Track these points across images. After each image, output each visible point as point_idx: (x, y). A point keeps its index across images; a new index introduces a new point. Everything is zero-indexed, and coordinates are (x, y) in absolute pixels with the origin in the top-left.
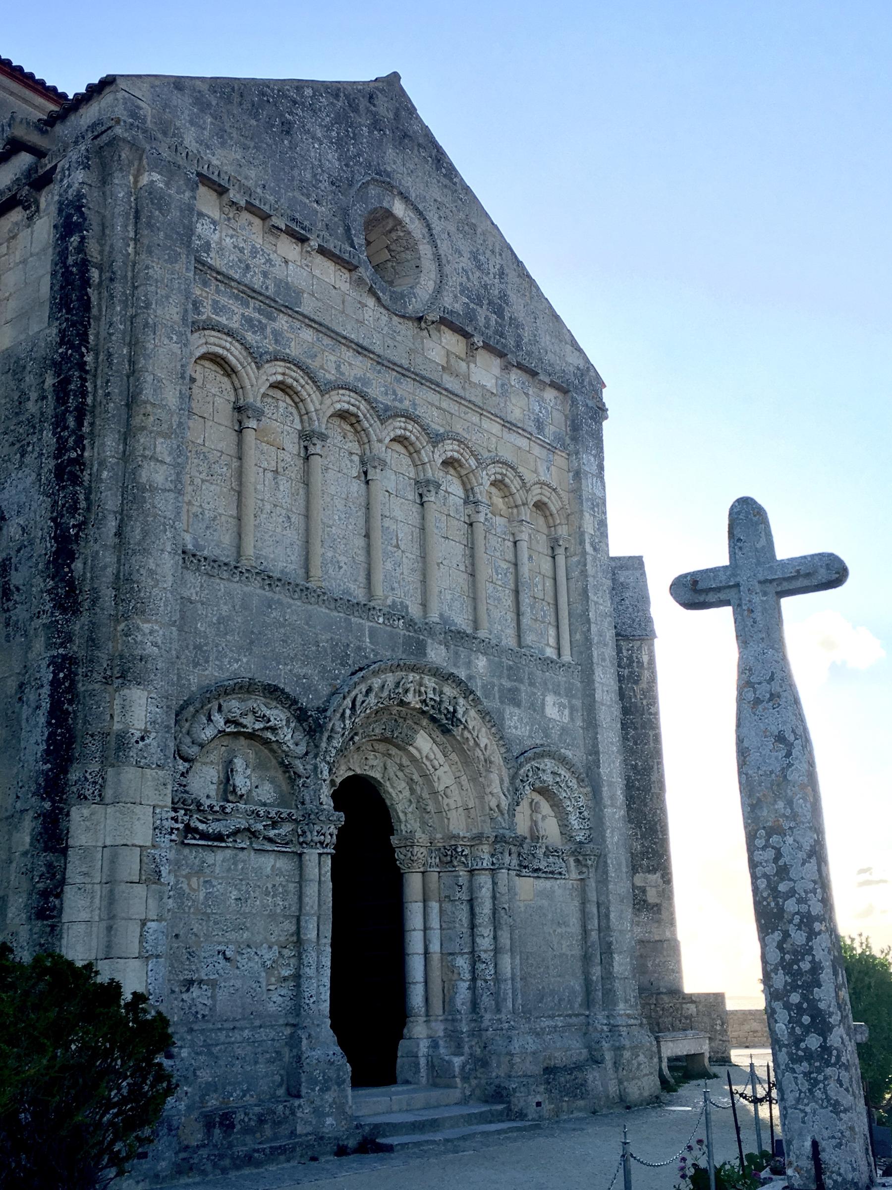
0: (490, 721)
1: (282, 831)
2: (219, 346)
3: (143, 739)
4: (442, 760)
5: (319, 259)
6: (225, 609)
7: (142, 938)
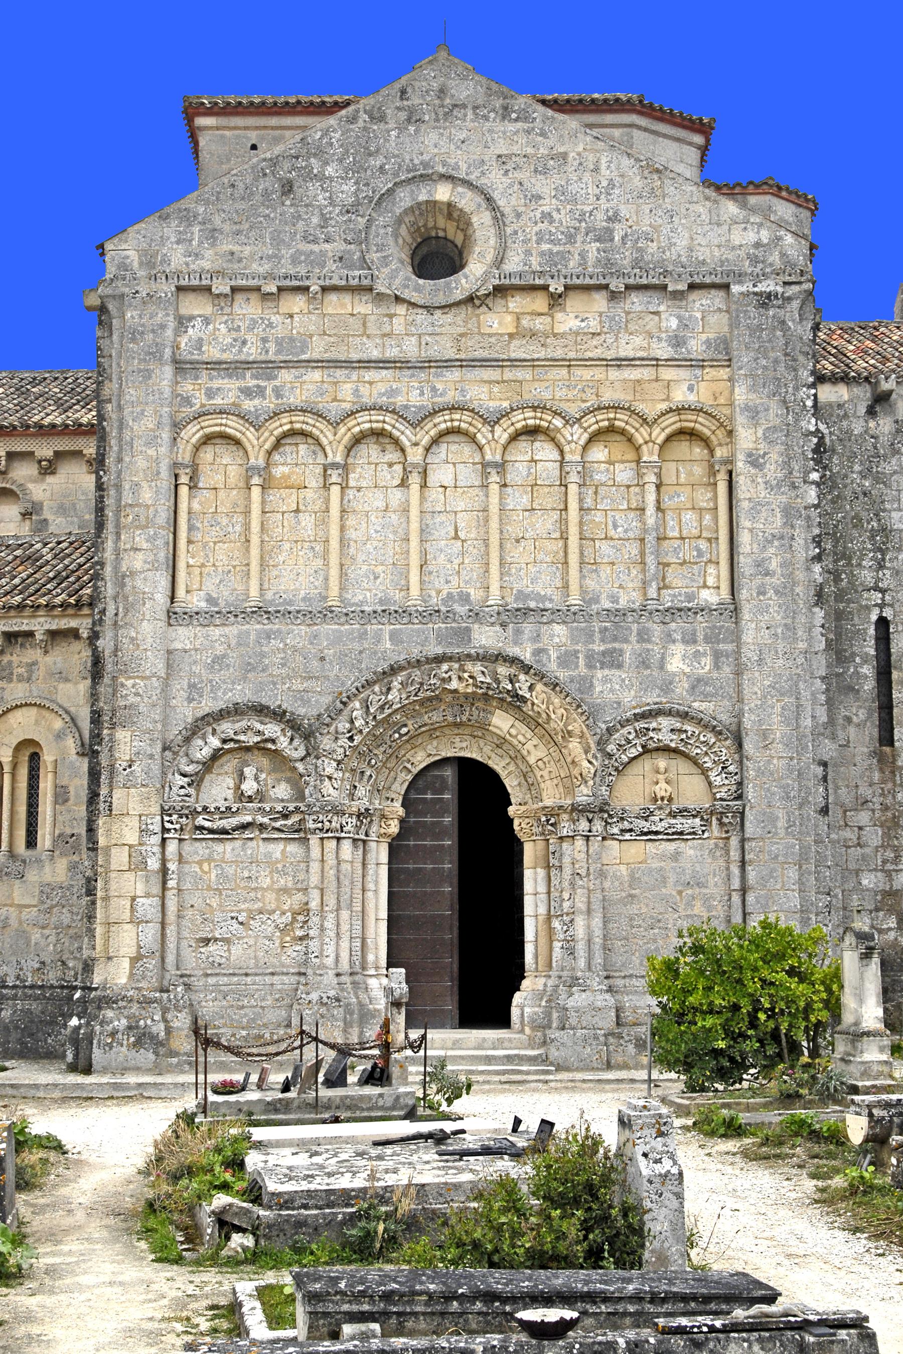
1: (289, 822)
2: (216, 425)
3: (130, 766)
4: (529, 734)
5: (333, 297)
6: (220, 649)
7: (133, 909)
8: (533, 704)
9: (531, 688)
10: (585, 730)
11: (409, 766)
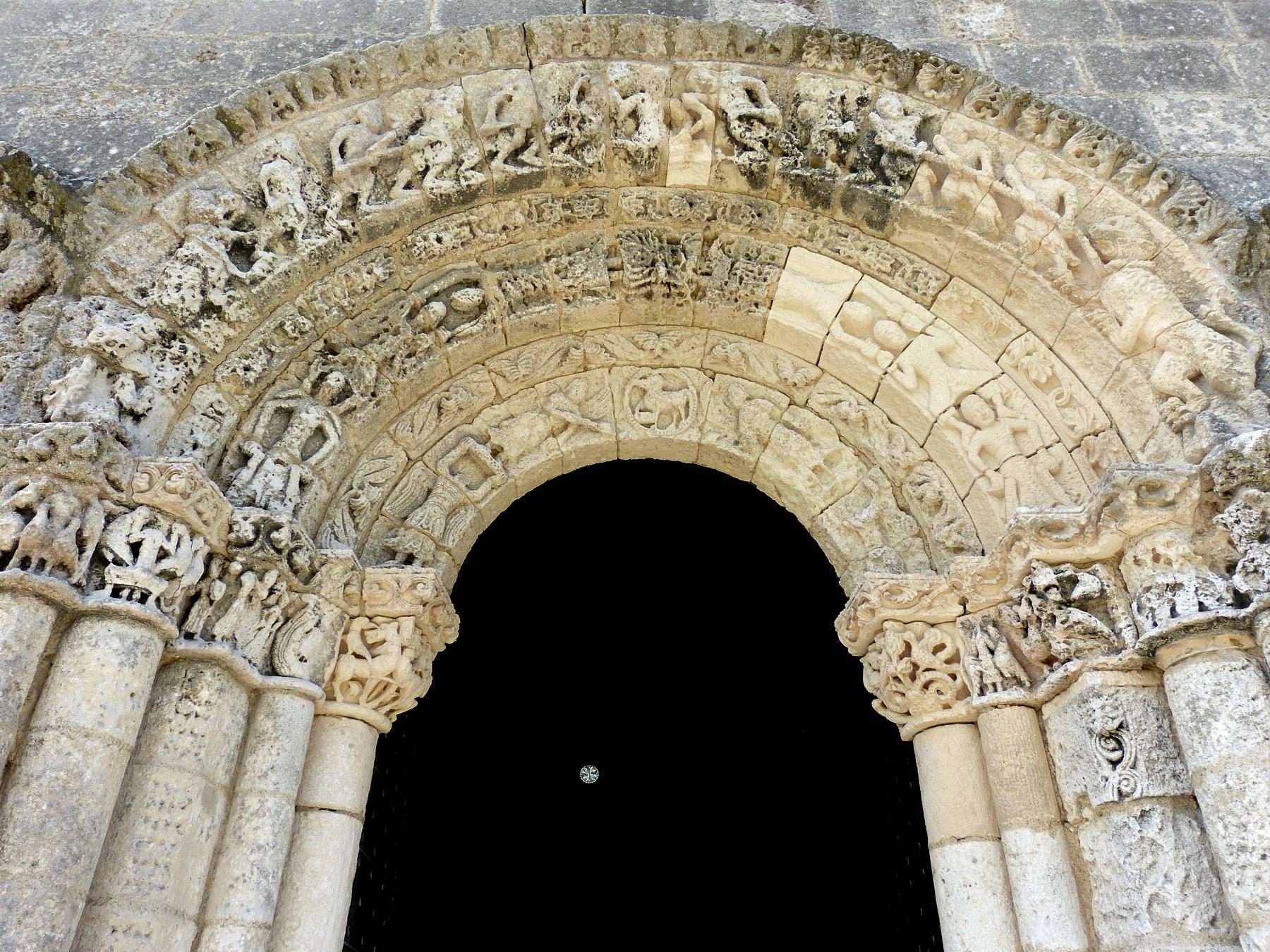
0: (1045, 122)
4: (917, 316)
8: (942, 172)
9: (924, 130)
10: (1163, 232)
11: (484, 452)
